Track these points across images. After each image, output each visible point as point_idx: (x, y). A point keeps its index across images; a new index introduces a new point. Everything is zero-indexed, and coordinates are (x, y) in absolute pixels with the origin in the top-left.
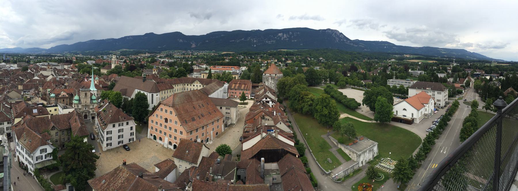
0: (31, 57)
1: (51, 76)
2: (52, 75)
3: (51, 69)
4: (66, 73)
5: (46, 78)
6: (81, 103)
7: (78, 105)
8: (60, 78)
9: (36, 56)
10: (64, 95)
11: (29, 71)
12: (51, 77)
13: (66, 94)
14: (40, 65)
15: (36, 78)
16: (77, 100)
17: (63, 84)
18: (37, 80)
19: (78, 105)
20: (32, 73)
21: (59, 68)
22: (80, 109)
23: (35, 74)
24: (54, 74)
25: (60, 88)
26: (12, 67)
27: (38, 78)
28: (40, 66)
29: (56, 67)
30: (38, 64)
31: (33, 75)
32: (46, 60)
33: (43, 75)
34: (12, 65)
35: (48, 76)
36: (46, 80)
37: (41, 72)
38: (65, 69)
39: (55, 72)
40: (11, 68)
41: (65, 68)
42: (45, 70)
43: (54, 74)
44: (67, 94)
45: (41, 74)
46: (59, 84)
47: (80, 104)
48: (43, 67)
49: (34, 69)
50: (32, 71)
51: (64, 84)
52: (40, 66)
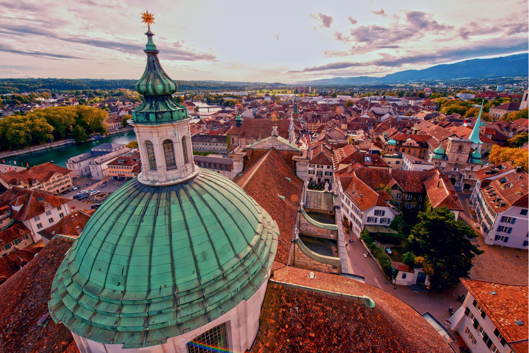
0: (355, 89)
1: (388, 115)
2: (390, 113)
3: (389, 104)
4: (412, 111)
5: (379, 118)
6: (447, 159)
7: (441, 162)
8: (403, 119)
9: (362, 87)
10: (411, 144)
11: (354, 106)
12: (387, 116)
13: (415, 142)
14: (368, 99)
15: (365, 116)
16: (440, 154)
17: (409, 128)
18: (366, 119)
19: (441, 162)
20: (359, 109)
21: (399, 103)
22: (443, 168)
23: (362, 111)
24: (393, 113)
25: (405, 132)
26: (331, 101)
27: (368, 117)
28: (369, 100)
29: (396, 102)
30: (366, 98)
31: (360, 111)
32: (377, 92)
33: (374, 113)
34: (331, 99)
35: (383, 115)
36: (379, 119)
37: (372, 109)
38: (410, 105)
39: (394, 109)
40: (330, 103)
41: (410, 103)
42: (378, 105)
43: (393, 113)
44: (417, 143)
45: (373, 111)
46: (403, 127)
47: (445, 160)
48: (373, 102)
49: (362, 104)
50: (358, 107)
51: (410, 127)
52: (369, 100)
